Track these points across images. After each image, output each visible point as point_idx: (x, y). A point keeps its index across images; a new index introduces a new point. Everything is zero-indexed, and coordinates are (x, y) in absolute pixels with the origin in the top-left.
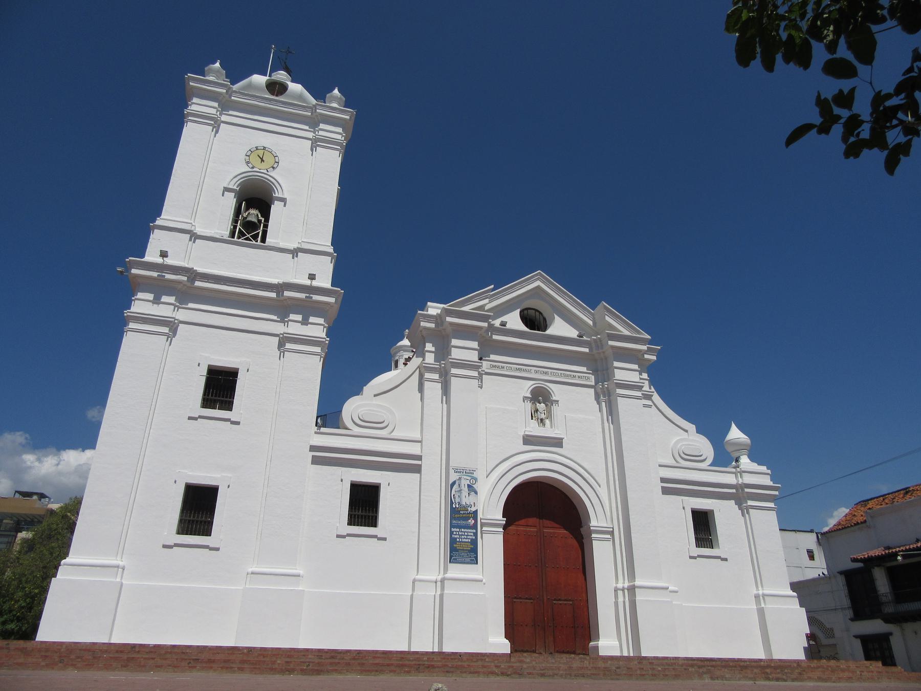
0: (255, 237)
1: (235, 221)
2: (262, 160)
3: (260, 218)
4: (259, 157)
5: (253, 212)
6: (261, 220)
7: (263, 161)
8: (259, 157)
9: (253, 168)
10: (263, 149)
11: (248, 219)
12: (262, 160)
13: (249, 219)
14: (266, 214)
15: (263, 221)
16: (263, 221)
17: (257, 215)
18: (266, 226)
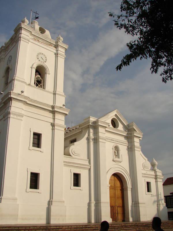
9: (39, 61)
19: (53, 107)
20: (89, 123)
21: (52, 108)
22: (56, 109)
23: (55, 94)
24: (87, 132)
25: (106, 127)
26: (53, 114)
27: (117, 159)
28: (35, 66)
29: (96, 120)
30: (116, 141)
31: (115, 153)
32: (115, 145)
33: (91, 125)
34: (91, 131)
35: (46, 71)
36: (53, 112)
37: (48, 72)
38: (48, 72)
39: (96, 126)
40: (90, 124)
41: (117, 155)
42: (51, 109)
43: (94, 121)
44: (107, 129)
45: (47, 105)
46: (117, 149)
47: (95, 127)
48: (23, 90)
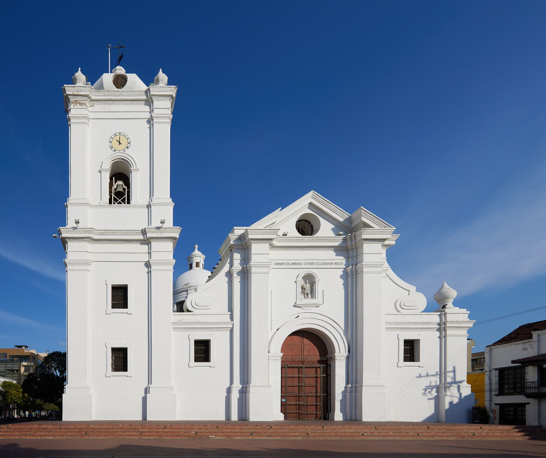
0: (123, 201)
1: (110, 192)
2: (120, 144)
3: (124, 187)
4: (118, 141)
5: (120, 183)
6: (125, 188)
7: (121, 144)
8: (118, 141)
9: (115, 150)
10: (119, 135)
11: (117, 190)
12: (120, 144)
13: (118, 190)
14: (127, 182)
15: (126, 189)
16: (126, 189)
17: (122, 185)
18: (129, 192)
19: (144, 232)
20: (230, 240)
21: (143, 235)
22: (149, 235)
23: (149, 206)
24: (228, 261)
25: (271, 239)
26: (148, 244)
27: (310, 301)
28: (108, 166)
29: (243, 231)
30: (306, 264)
31: (303, 288)
32: (303, 273)
33: (233, 245)
34: (237, 256)
35: (131, 167)
36: (147, 241)
37: (135, 168)
38: (135, 168)
39: (246, 244)
40: (232, 242)
41: (309, 292)
42: (141, 237)
43: (240, 235)
44: (275, 243)
45: (134, 232)
46: (310, 279)
47: (245, 246)
48: (77, 219)
